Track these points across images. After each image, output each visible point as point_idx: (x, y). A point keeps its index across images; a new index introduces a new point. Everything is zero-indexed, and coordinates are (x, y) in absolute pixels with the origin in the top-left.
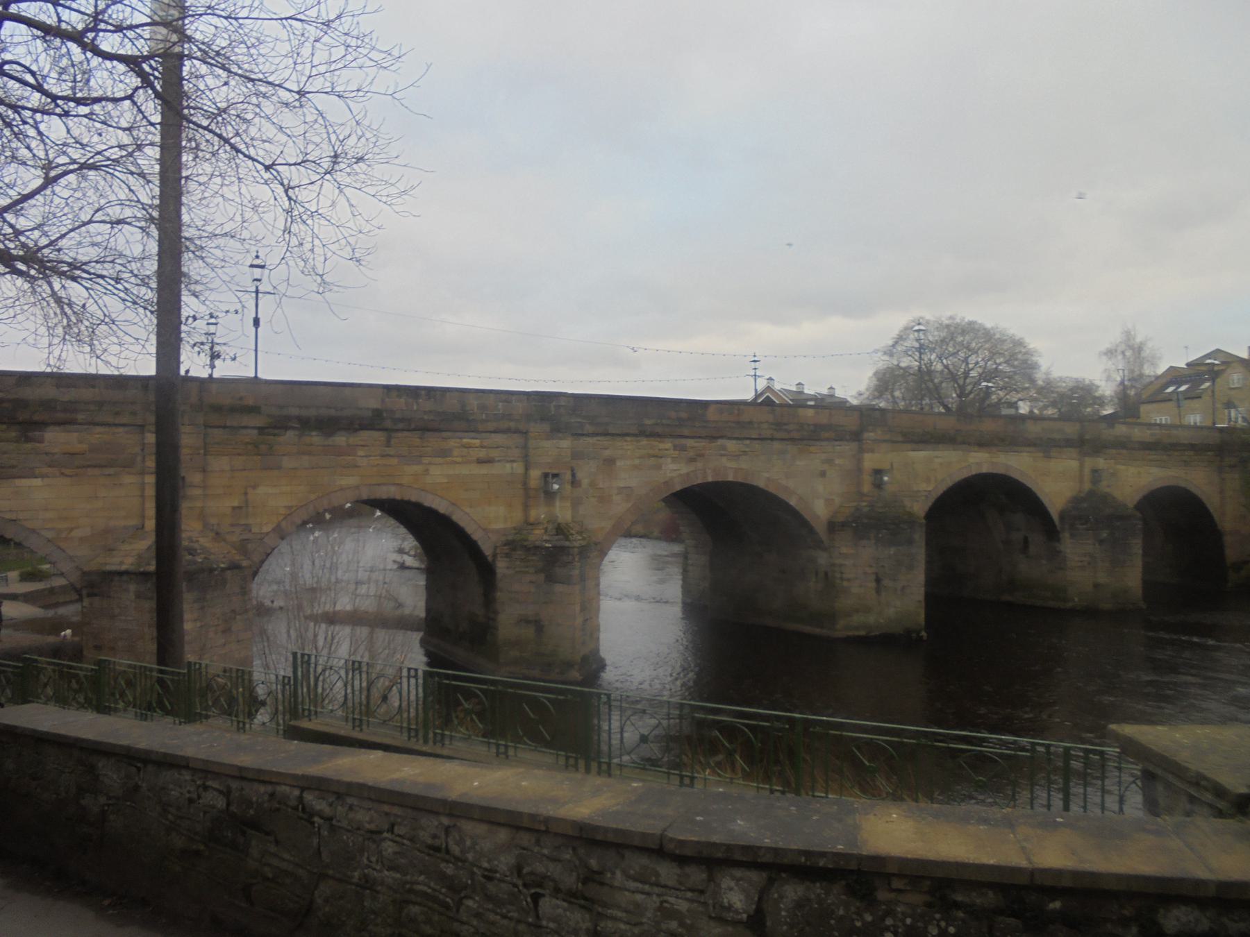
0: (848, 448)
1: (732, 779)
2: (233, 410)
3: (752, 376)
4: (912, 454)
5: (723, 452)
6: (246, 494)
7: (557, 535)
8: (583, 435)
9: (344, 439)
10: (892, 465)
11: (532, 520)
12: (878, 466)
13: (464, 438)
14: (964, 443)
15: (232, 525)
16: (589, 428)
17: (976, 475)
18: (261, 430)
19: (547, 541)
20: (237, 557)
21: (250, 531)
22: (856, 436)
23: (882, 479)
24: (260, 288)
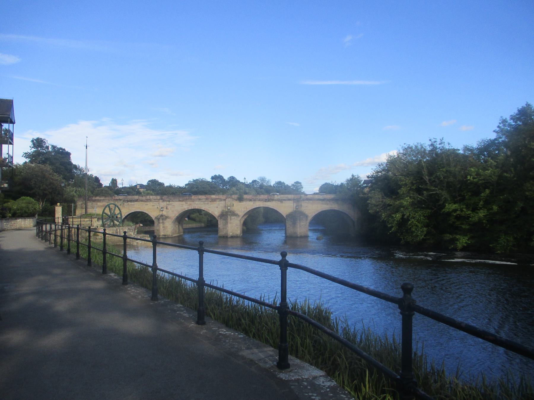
0: (223, 202)
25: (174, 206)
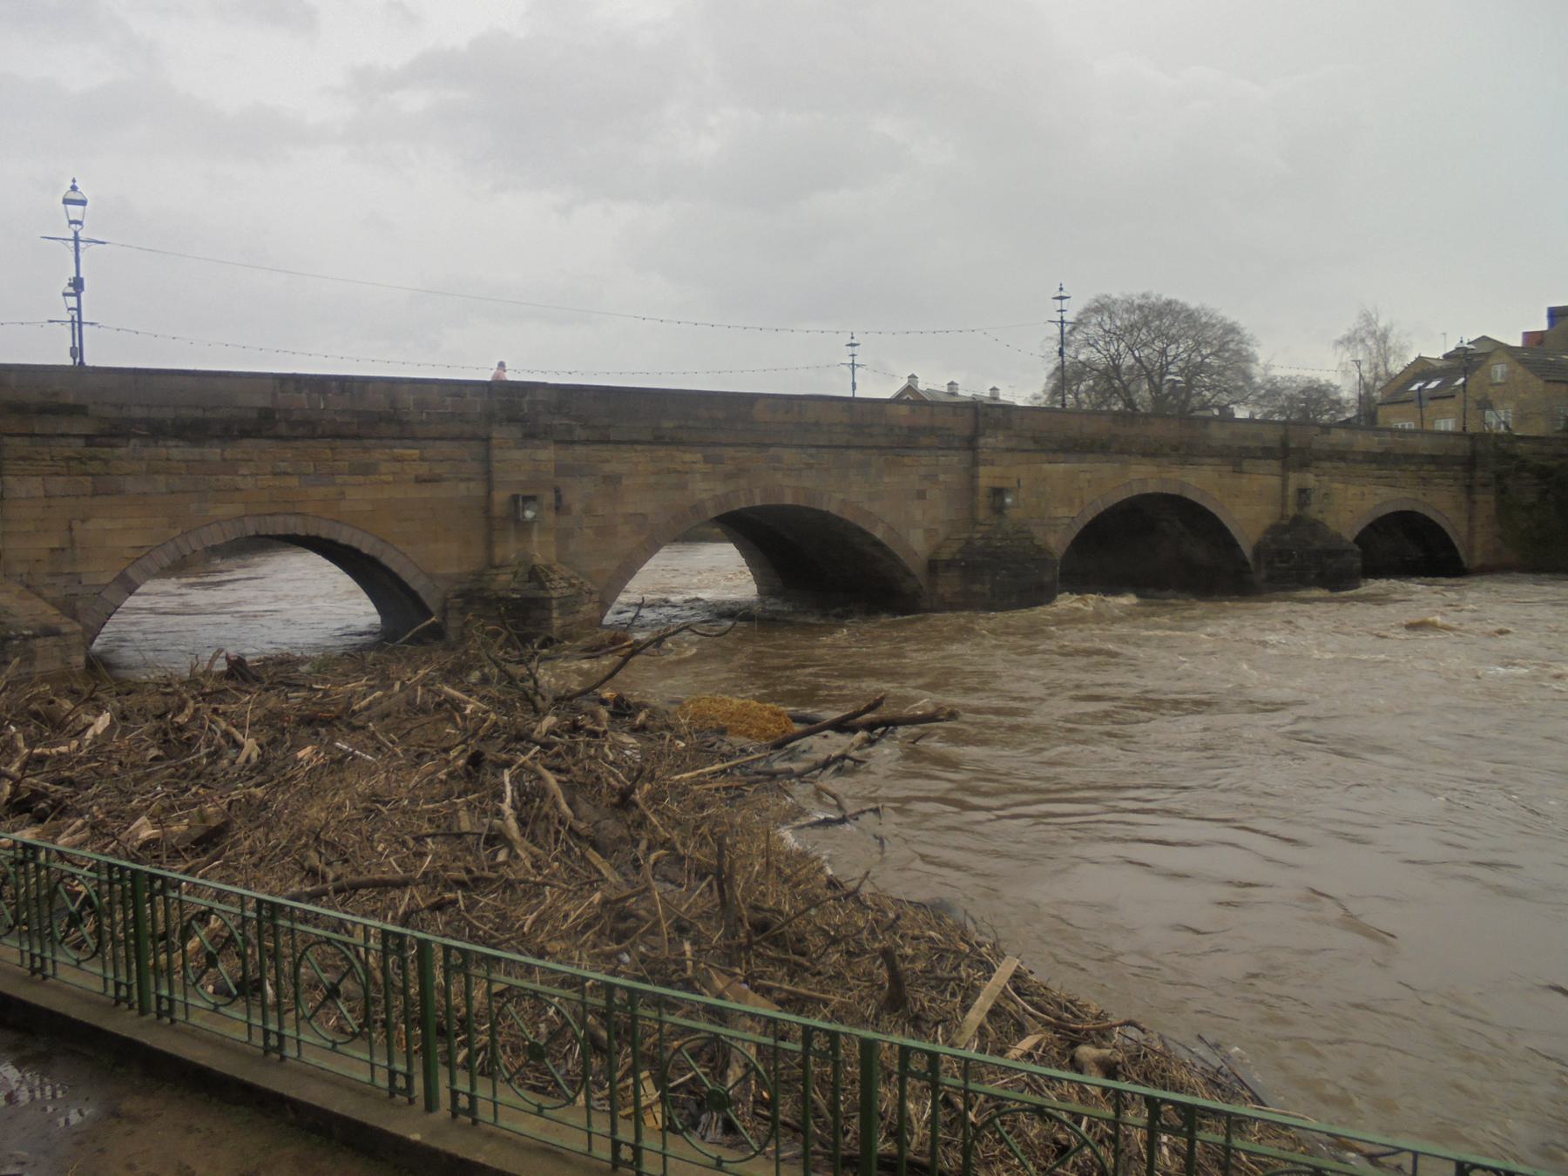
0: (955, 459)
1: (334, 1043)
2: (45, 410)
3: (848, 365)
4: (1047, 467)
5: (776, 465)
6: (70, 529)
7: (529, 582)
8: (573, 442)
9: (218, 451)
10: (1019, 482)
11: (497, 561)
12: (998, 484)
13: (395, 447)
14: (1121, 452)
15: (52, 575)
16: (579, 433)
17: (1138, 496)
18: (89, 439)
19: (514, 590)
20: (56, 620)
21: (80, 583)
22: (971, 444)
23: (1003, 500)
24: (80, 234)
25: (612, 480)
